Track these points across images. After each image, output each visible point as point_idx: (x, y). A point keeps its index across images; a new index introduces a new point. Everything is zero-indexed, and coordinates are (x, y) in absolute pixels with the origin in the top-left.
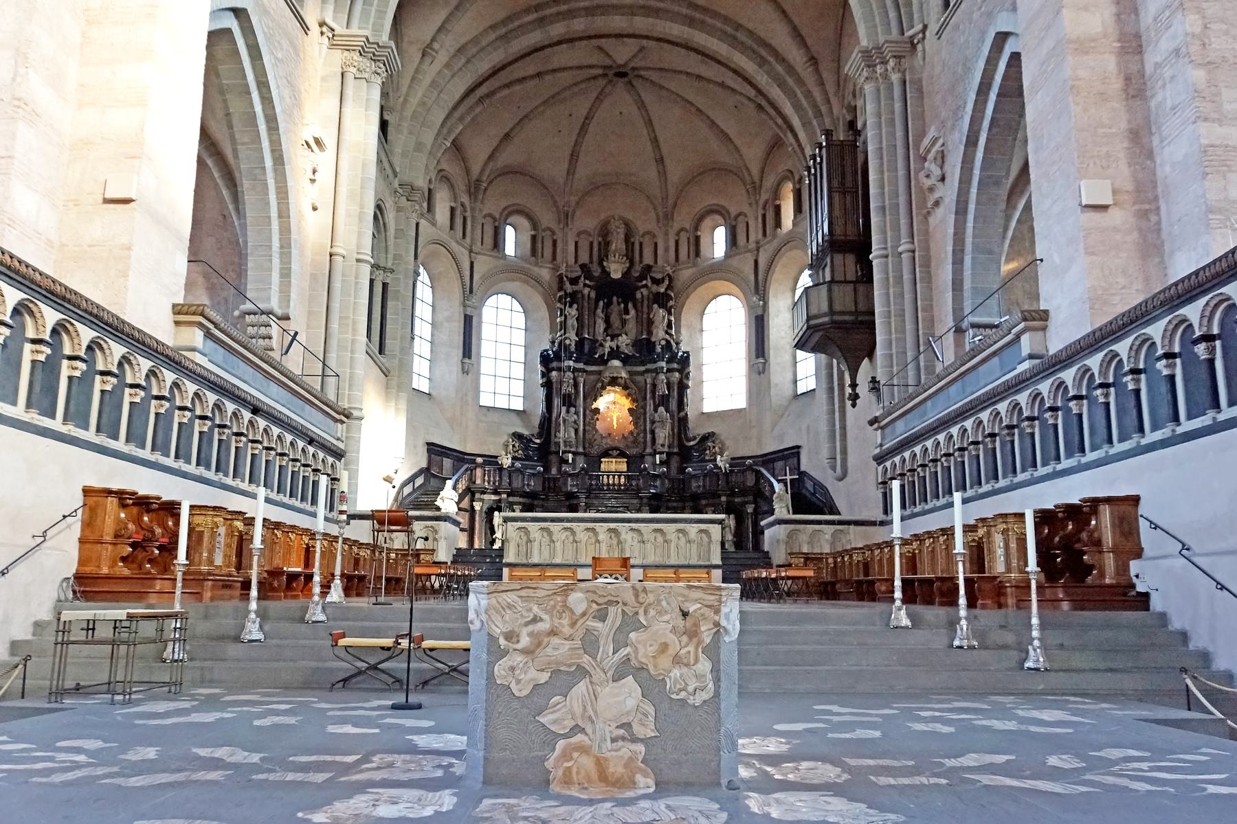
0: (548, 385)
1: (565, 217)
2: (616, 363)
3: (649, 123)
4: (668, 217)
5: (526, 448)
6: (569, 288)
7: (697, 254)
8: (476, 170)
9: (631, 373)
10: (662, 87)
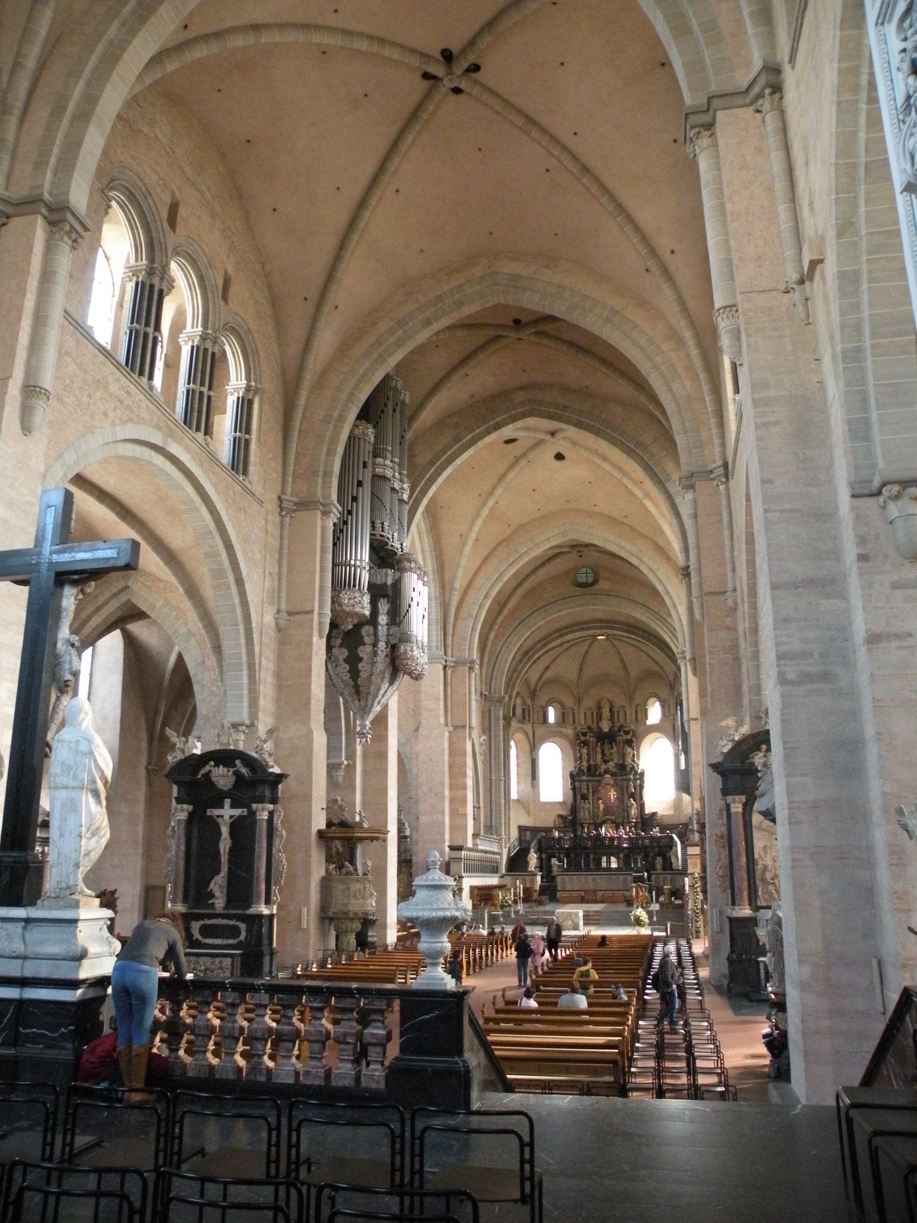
0: (574, 789)
1: (579, 701)
2: (608, 776)
3: (619, 653)
4: (630, 698)
5: (565, 823)
6: (582, 738)
7: (646, 718)
8: (532, 687)
9: (615, 780)
10: (622, 641)
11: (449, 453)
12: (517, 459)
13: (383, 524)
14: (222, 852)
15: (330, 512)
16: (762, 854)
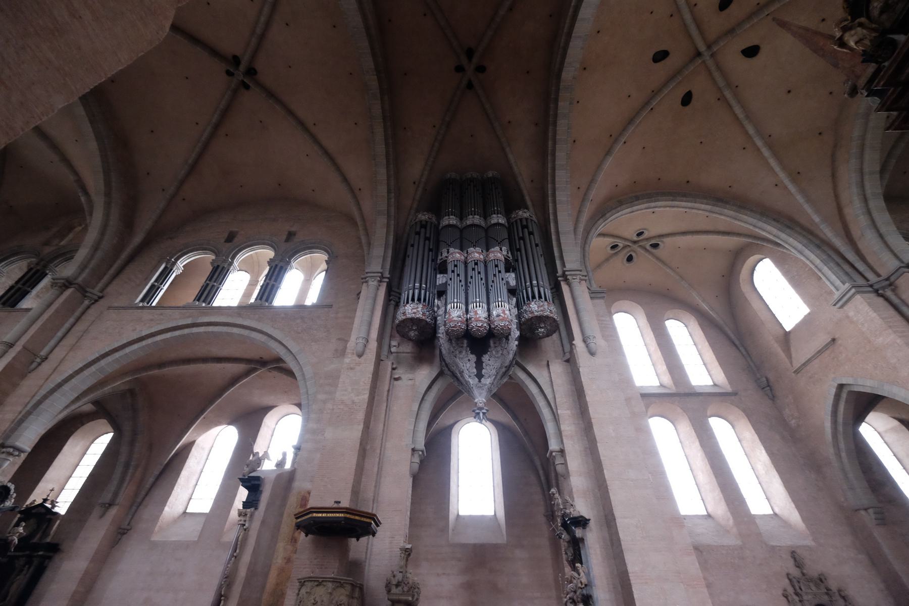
12: (722, 98)
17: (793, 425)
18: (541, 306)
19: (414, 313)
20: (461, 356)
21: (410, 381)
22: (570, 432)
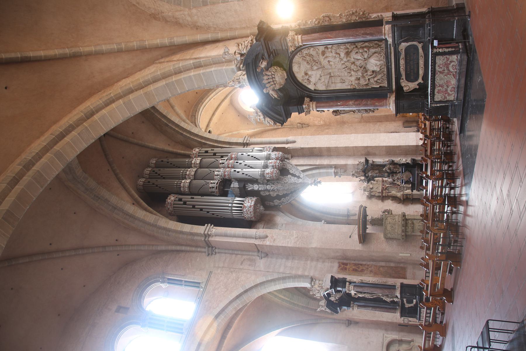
11: (174, 128)
13: (210, 188)
14: (372, 298)
15: (208, 234)
16: (347, 84)
17: (323, 123)
18: (267, 149)
19: (252, 201)
20: (287, 180)
21: (283, 226)
22: (328, 161)
